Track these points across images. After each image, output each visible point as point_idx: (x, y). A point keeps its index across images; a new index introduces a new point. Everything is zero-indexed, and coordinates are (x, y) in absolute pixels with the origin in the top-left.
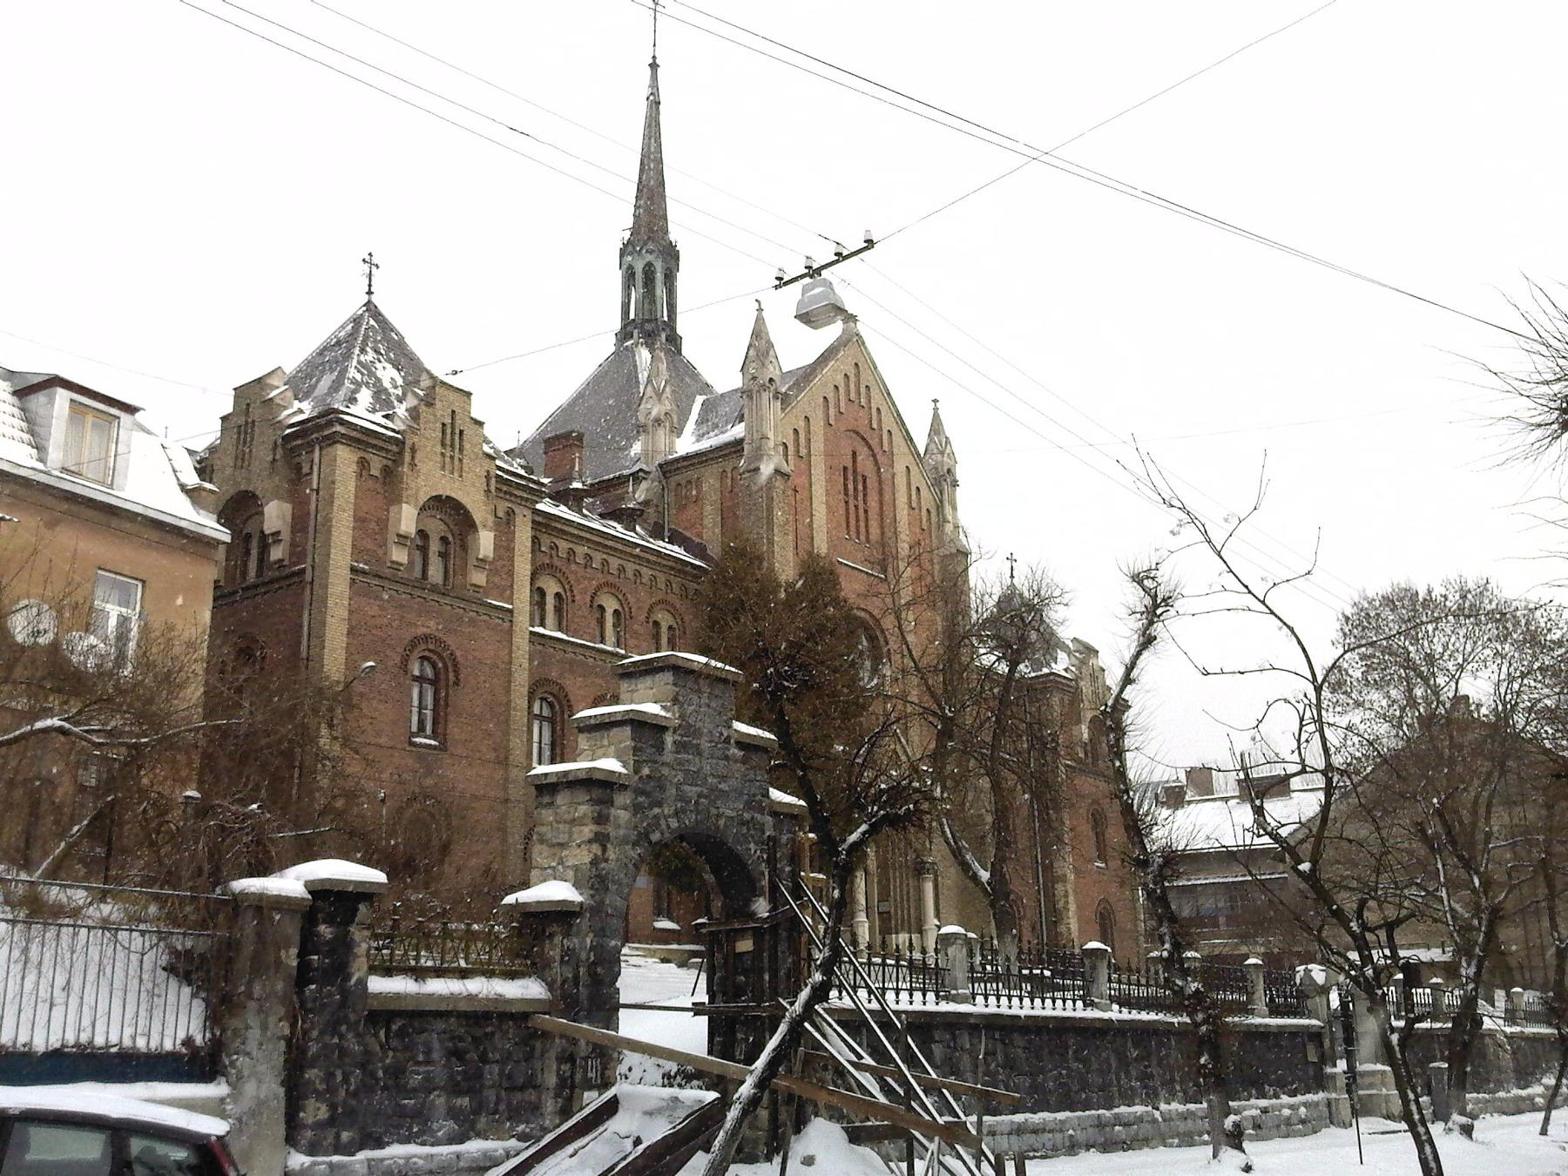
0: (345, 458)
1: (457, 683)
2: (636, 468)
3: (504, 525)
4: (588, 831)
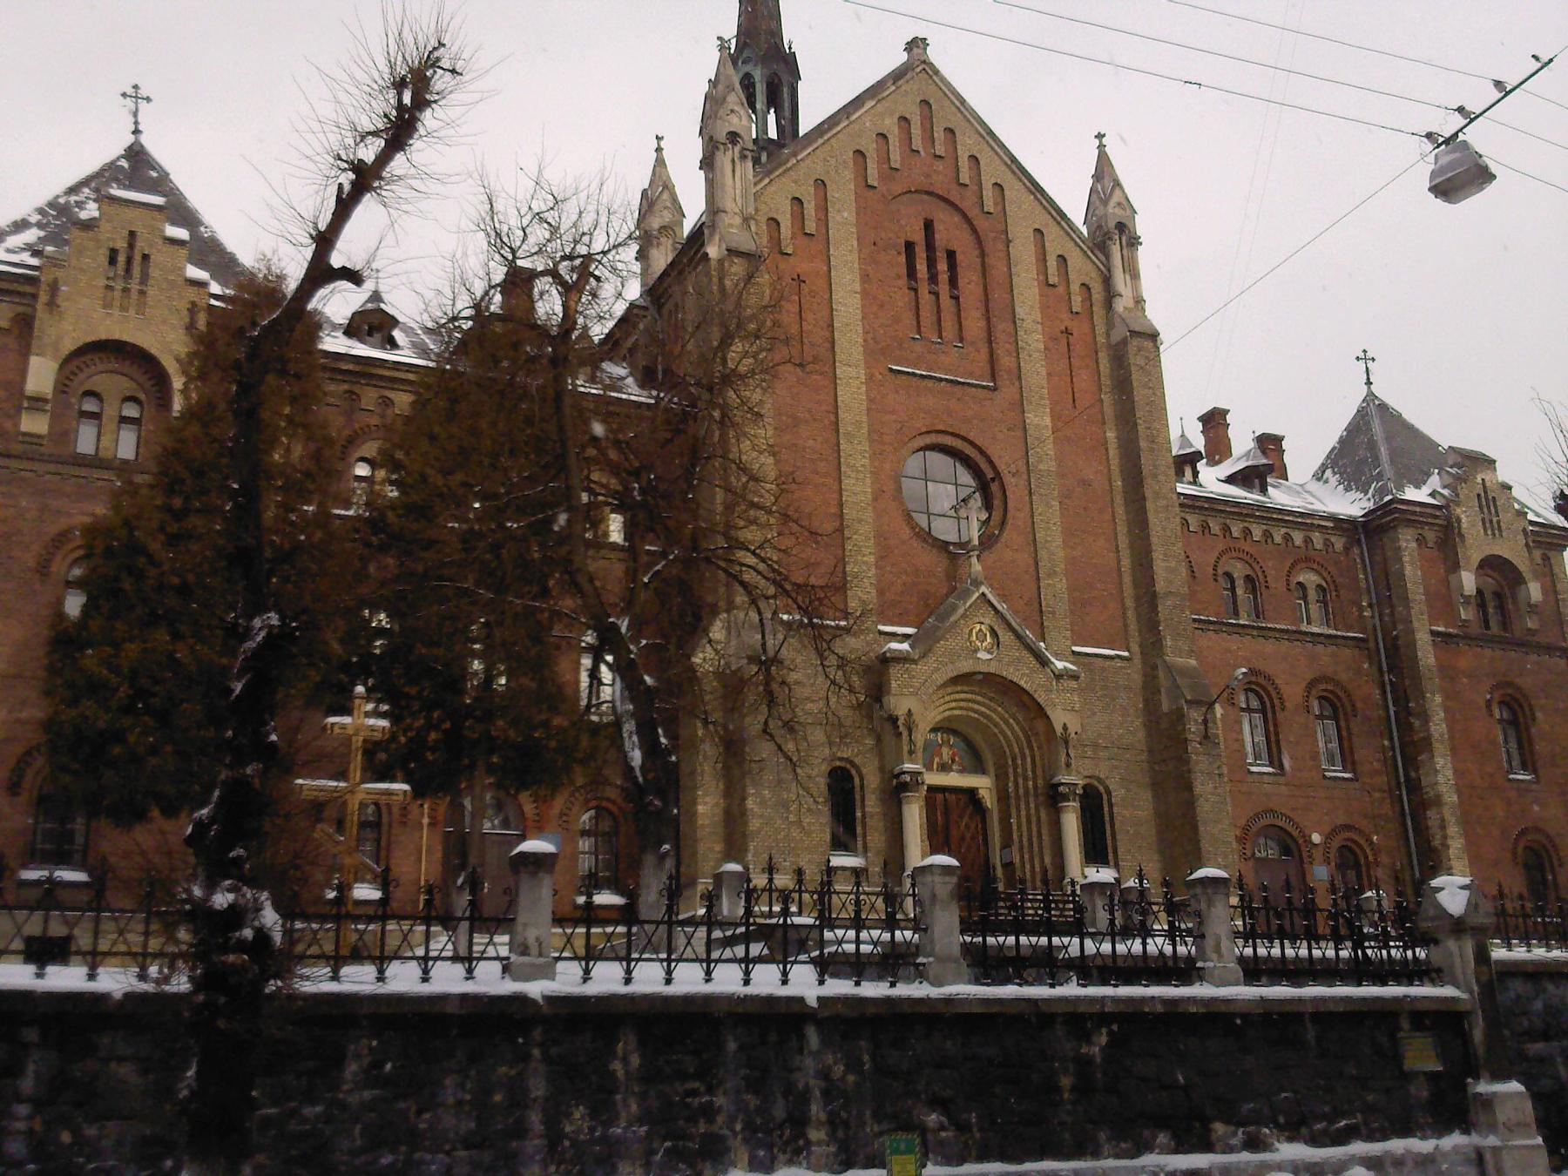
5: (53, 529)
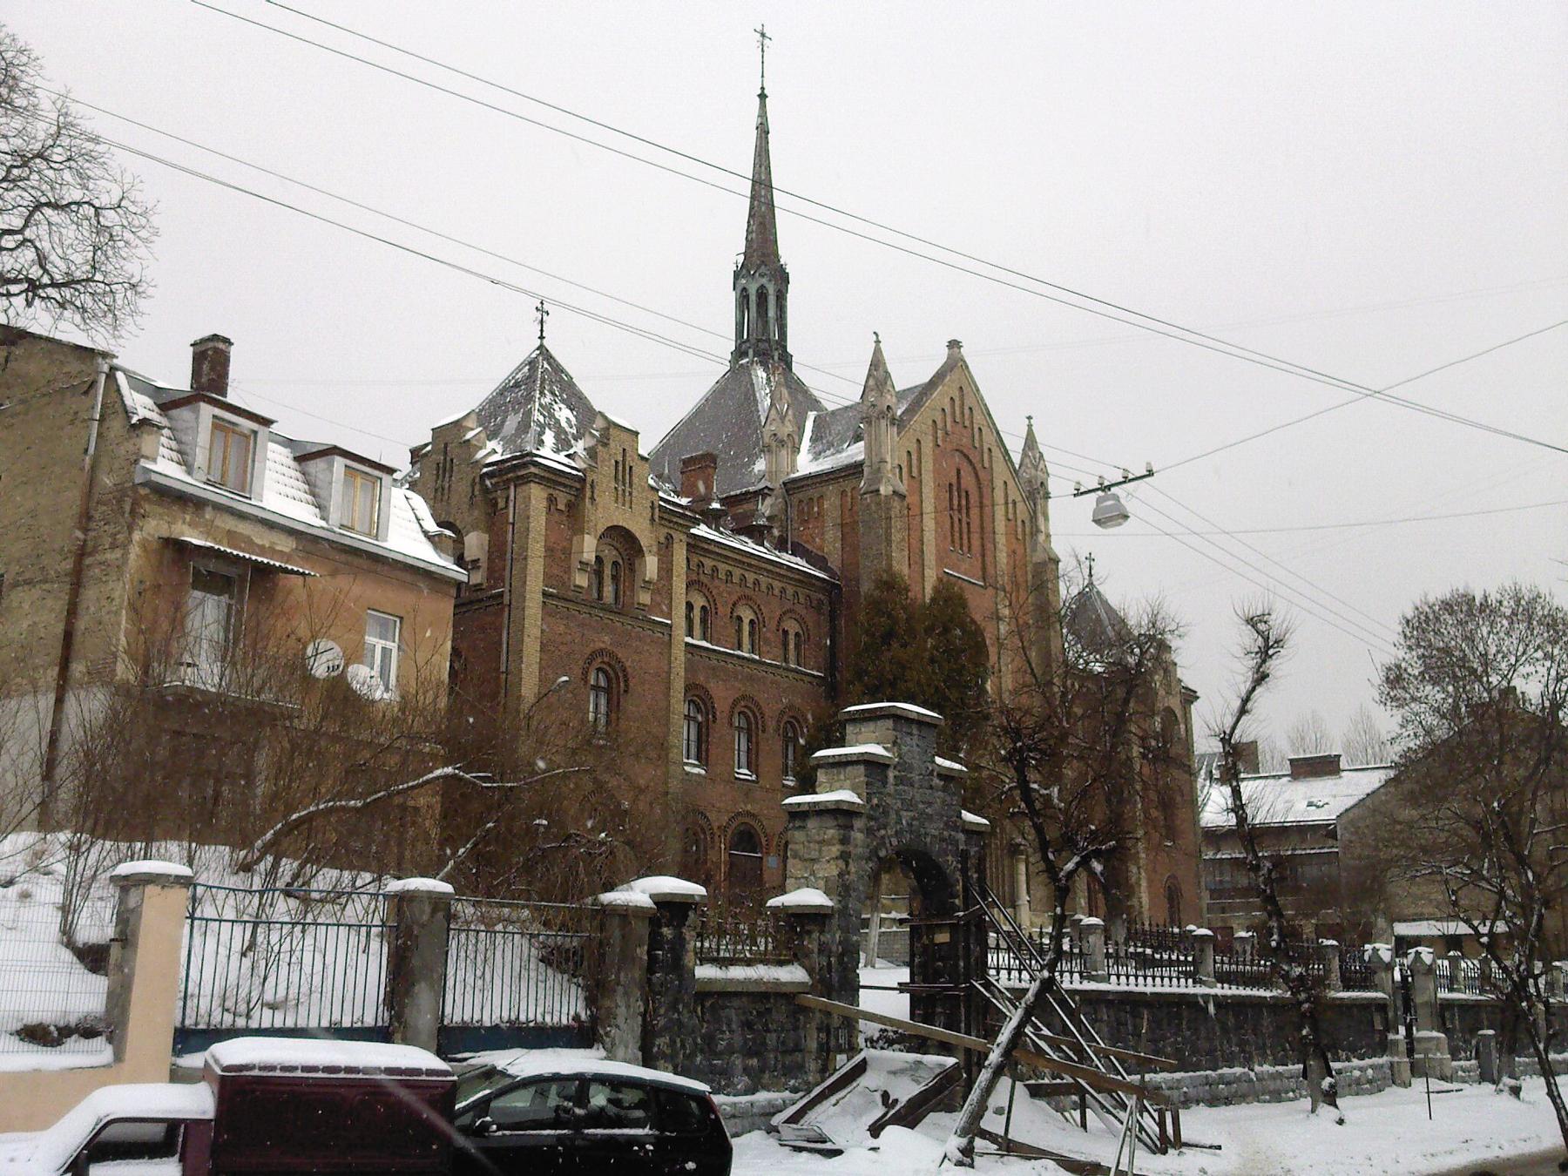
0: (537, 495)
2: (761, 486)
3: (665, 548)
4: (835, 850)
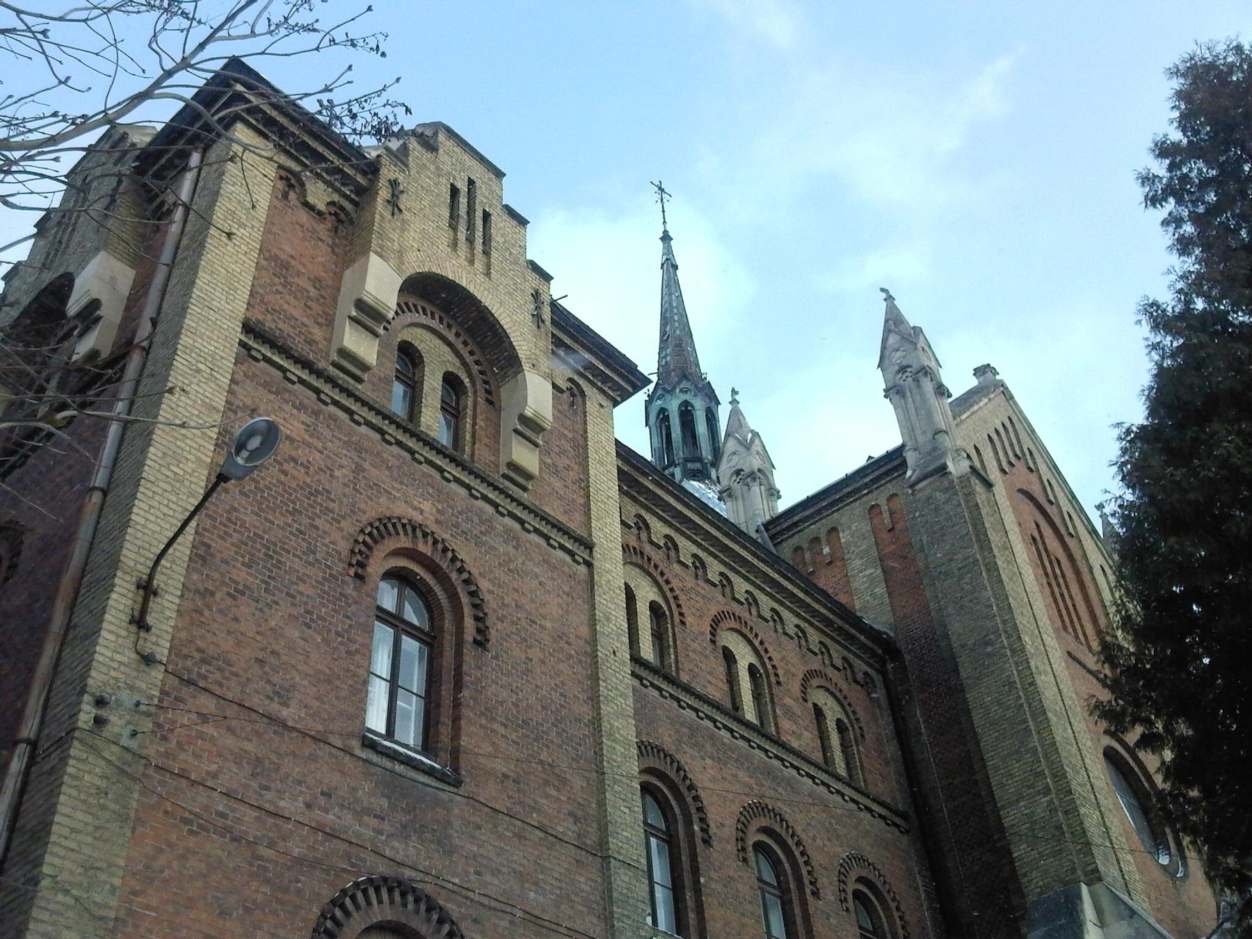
1: (481, 643)
5: (372, 509)
